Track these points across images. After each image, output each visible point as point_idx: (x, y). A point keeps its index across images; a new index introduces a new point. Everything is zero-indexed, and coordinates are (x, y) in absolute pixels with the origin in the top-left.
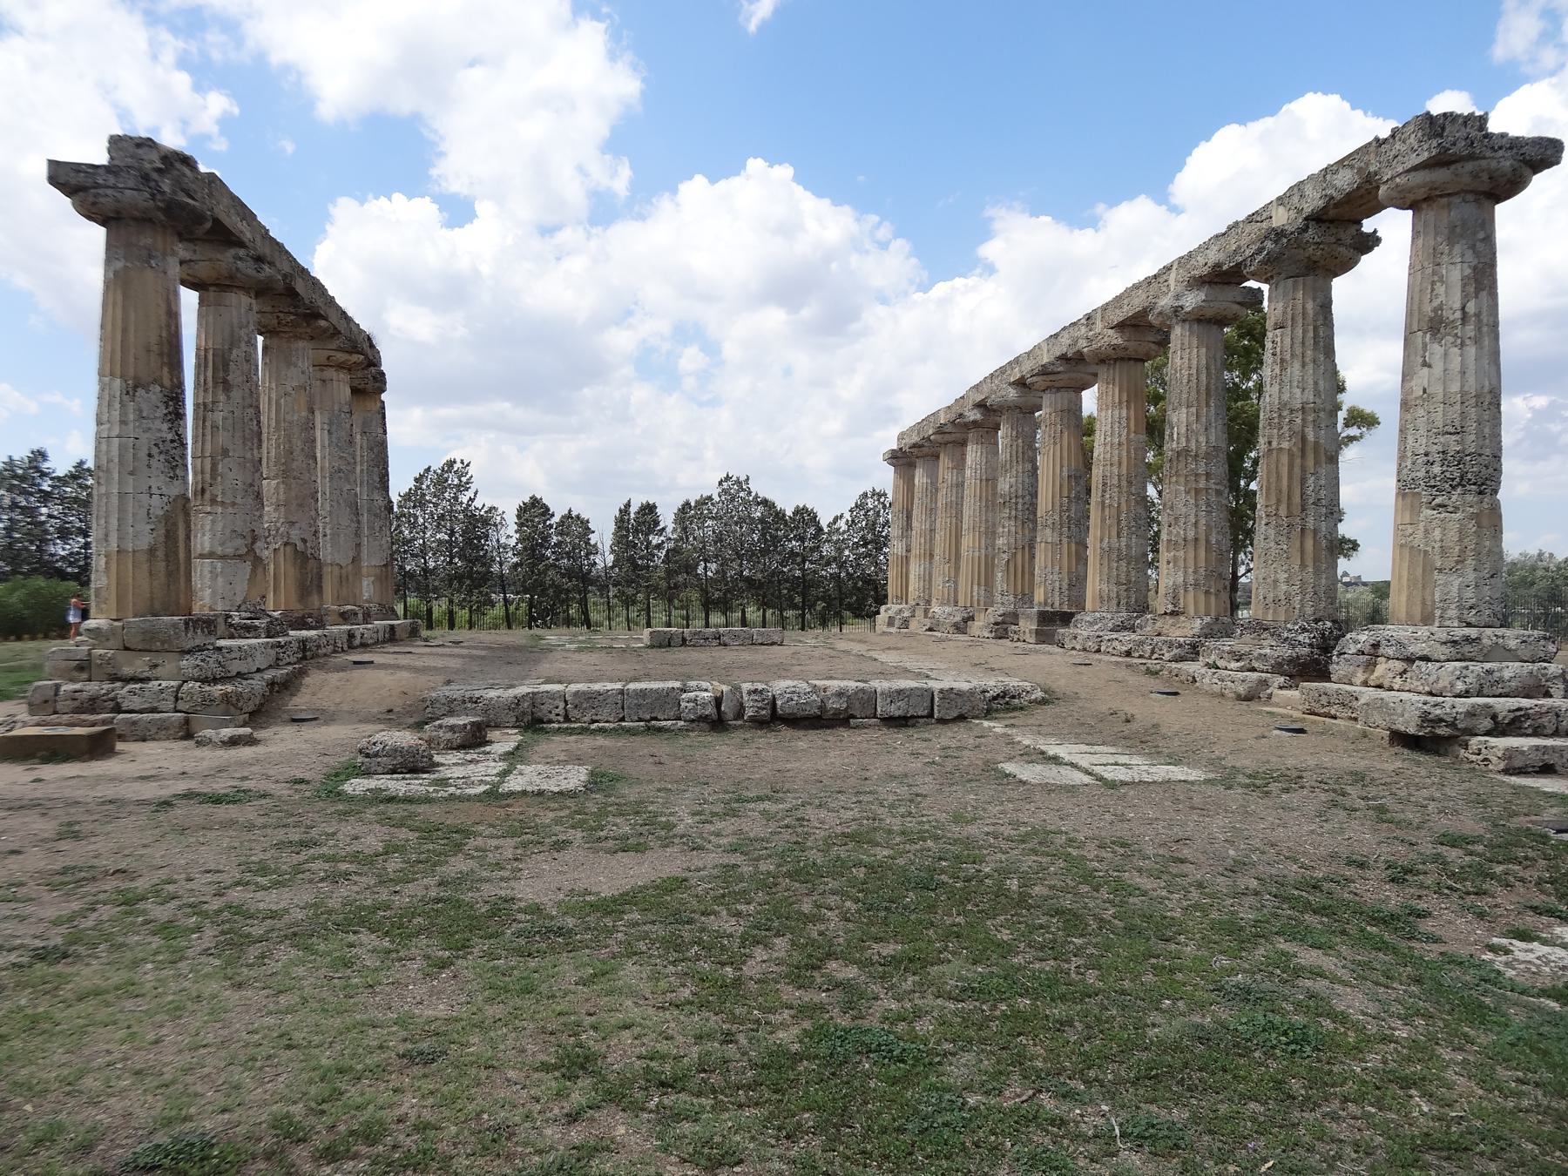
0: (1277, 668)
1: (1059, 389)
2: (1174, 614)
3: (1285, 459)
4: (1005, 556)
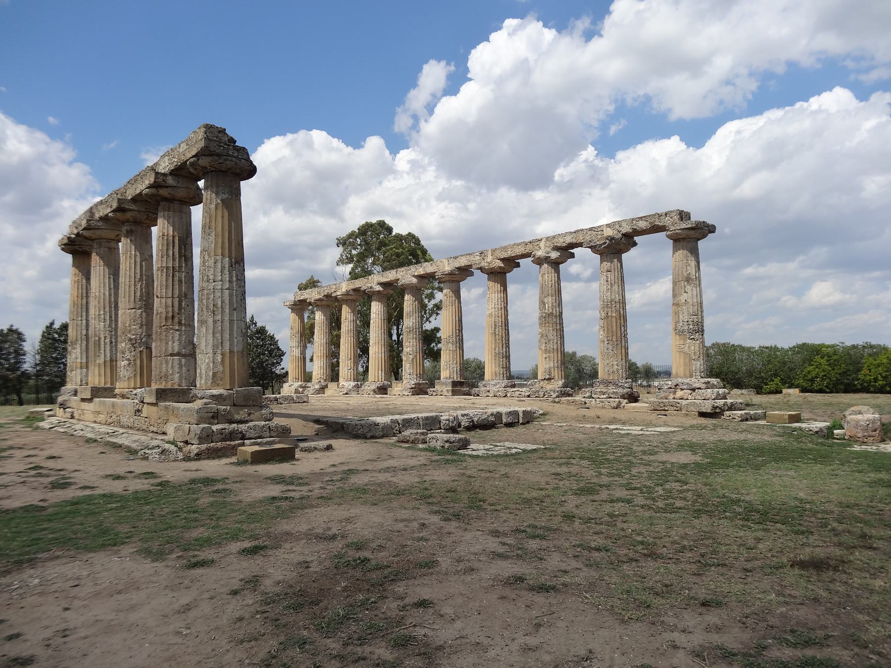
0: (623, 397)
1: (453, 281)
2: (549, 379)
3: (614, 320)
4: (411, 357)
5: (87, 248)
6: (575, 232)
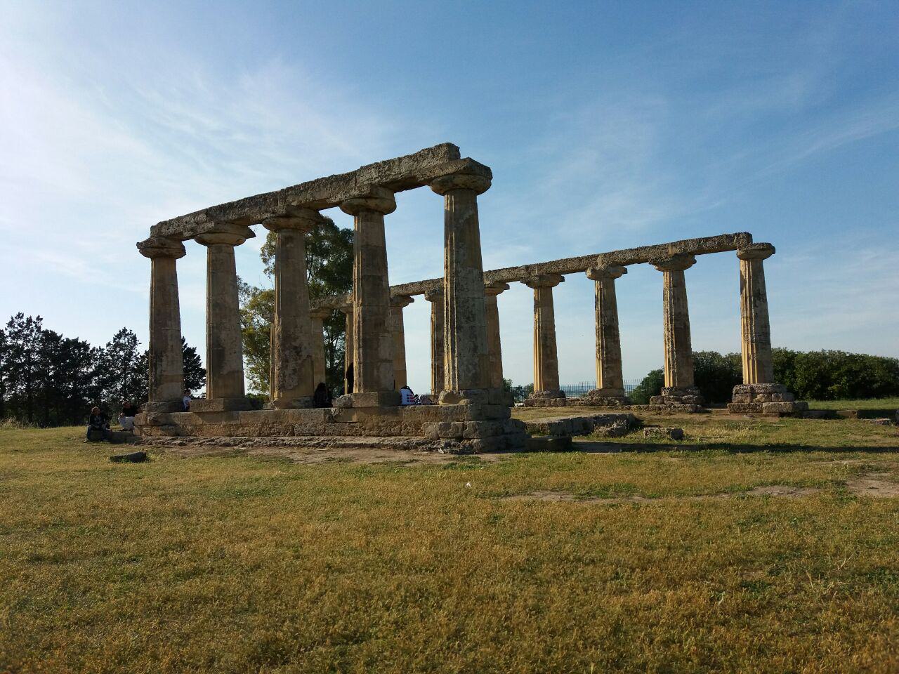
5: (173, 252)
6: (637, 249)
